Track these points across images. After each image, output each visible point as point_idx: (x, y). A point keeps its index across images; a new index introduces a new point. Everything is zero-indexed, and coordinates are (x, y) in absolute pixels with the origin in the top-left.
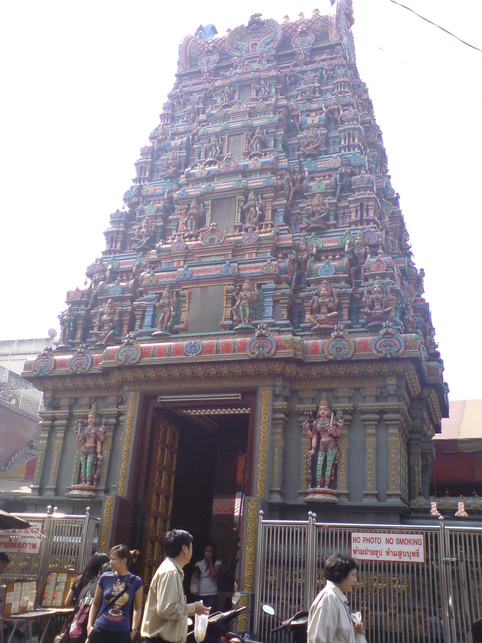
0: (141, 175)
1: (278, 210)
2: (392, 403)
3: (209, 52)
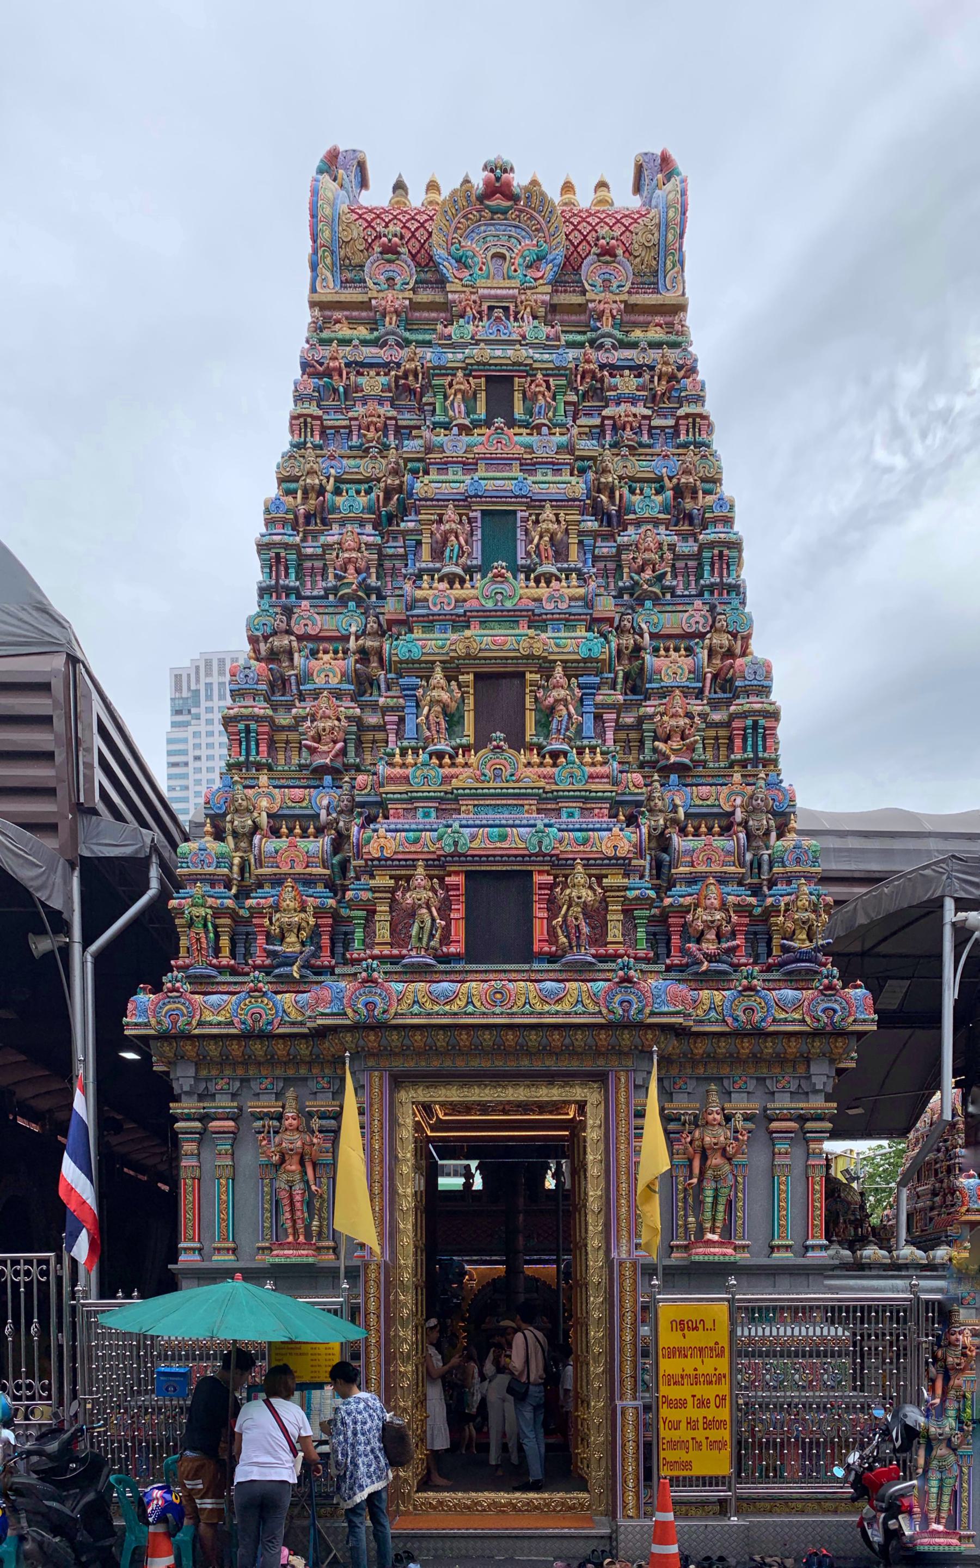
1: (605, 716)
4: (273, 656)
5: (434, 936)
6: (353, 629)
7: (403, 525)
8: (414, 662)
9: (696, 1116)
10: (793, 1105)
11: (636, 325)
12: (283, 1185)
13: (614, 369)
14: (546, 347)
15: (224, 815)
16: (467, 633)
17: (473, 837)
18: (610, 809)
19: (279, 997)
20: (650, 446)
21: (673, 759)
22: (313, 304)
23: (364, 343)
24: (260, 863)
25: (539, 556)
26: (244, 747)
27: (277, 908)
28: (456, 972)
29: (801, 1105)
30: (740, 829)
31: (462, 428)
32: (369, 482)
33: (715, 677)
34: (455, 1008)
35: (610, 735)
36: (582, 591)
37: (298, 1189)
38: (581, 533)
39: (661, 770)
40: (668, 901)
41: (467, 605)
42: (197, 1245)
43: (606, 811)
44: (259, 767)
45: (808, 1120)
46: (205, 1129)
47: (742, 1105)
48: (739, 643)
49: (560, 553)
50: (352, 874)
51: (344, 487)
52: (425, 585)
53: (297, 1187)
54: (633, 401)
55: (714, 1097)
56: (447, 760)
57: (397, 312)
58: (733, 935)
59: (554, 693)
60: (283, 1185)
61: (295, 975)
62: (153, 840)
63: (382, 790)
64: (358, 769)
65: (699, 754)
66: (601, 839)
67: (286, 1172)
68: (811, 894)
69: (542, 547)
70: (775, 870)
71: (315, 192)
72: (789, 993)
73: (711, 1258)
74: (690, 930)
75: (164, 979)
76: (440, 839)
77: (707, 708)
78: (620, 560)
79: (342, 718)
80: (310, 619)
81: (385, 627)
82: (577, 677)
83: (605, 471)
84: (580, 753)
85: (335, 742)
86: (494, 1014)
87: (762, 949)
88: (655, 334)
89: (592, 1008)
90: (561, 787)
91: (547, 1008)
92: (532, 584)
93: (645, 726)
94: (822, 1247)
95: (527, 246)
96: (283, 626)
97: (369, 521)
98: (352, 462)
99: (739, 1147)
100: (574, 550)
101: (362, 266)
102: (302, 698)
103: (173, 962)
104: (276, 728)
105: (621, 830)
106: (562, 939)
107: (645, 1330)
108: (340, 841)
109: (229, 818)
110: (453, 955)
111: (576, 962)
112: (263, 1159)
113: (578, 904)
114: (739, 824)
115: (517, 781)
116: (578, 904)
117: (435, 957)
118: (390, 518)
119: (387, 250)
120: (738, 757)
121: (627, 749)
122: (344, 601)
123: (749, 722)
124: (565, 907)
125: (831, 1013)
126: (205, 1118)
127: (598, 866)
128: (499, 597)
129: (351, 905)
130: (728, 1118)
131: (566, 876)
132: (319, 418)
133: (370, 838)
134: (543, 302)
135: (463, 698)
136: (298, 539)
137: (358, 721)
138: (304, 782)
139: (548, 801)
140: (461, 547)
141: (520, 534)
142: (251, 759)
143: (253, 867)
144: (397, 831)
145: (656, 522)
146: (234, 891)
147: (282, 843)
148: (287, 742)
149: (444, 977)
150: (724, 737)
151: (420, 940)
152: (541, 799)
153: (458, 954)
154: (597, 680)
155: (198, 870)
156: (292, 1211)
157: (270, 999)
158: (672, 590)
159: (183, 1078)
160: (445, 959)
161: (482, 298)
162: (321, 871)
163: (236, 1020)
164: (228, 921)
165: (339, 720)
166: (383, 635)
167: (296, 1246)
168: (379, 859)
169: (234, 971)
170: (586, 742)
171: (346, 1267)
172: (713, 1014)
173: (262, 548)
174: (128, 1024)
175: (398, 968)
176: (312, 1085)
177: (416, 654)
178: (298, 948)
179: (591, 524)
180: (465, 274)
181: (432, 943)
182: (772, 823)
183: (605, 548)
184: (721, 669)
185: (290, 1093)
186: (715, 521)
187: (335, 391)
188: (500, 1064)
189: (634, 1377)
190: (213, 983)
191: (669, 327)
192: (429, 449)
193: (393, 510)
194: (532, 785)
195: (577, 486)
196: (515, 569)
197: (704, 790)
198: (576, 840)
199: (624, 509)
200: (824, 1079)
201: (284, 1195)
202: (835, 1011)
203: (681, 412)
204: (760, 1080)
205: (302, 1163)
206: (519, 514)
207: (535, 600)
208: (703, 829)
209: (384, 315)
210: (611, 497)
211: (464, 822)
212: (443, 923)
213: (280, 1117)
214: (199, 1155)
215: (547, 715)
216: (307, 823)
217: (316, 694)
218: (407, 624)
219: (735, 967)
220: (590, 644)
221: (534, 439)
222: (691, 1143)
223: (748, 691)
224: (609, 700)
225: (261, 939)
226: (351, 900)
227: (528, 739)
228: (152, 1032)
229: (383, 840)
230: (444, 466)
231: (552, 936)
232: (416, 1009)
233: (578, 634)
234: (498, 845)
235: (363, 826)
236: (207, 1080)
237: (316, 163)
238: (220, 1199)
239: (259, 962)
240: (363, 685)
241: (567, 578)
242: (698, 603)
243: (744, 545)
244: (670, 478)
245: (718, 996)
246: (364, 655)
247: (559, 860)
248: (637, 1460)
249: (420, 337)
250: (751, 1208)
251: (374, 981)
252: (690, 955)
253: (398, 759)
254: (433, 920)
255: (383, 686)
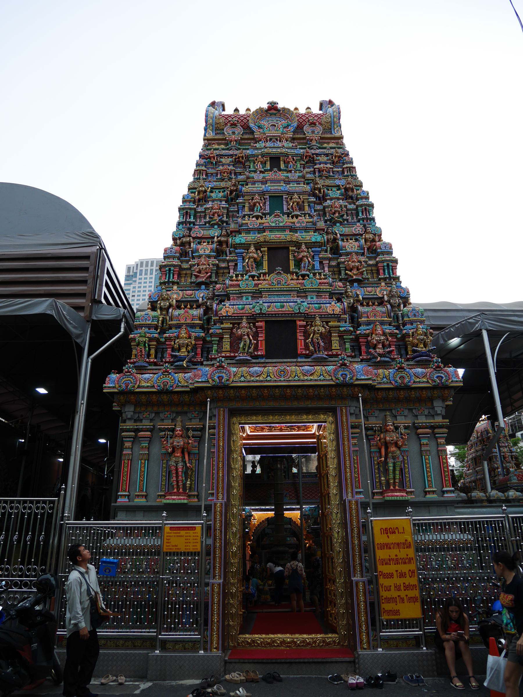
0: (186, 219)
2: (439, 420)
3: (234, 125)
4: (183, 244)
5: (251, 348)
6: (216, 234)
7: (237, 201)
8: (242, 244)
9: (380, 427)
10: (428, 421)
11: (325, 143)
12: (173, 463)
13: (317, 155)
14: (292, 148)
15: (157, 301)
16: (264, 234)
17: (269, 307)
18: (329, 296)
19: (177, 375)
20: (334, 176)
21: (354, 277)
22: (204, 140)
23: (223, 149)
24: (171, 319)
25: (293, 209)
26: (167, 276)
27: (178, 337)
28: (261, 363)
29: (432, 421)
30: (387, 303)
31: (261, 172)
32: (224, 189)
33: (368, 249)
34: (261, 378)
35: (326, 269)
36: (311, 220)
37: (180, 465)
38: (308, 202)
39: (349, 282)
40: (358, 332)
41: (264, 225)
42: (127, 493)
43: (328, 297)
44: (173, 283)
45: (436, 428)
46: (136, 435)
47: (402, 422)
48: (377, 237)
49: (301, 208)
50: (213, 323)
51: (214, 190)
52: (246, 219)
53: (180, 464)
54: (326, 163)
55: (389, 418)
56: (256, 278)
57: (236, 141)
58: (390, 346)
59: (302, 254)
60: (173, 463)
61: (185, 365)
62: (124, 312)
63: (227, 290)
64: (216, 283)
65: (365, 275)
66: (327, 307)
67: (175, 457)
68: (423, 328)
69: (294, 206)
70: (405, 319)
71: (207, 111)
72: (420, 370)
73: (396, 498)
74: (370, 344)
75: (124, 368)
76: (254, 307)
77: (367, 260)
78: (325, 211)
79: (210, 264)
80: (198, 232)
81: (229, 233)
82: (311, 248)
83: (317, 184)
84: (314, 274)
85: (207, 273)
86: (280, 381)
87: (403, 352)
88: (332, 145)
89: (328, 378)
90: (307, 287)
91: (306, 378)
92: (290, 218)
93: (341, 266)
94: (451, 491)
95: (284, 122)
96: (187, 234)
97: (224, 200)
98: (218, 183)
99: (403, 442)
100: (307, 208)
101: (223, 129)
102: (193, 258)
103: (128, 361)
104: (181, 268)
105: (335, 303)
106: (311, 348)
107: (364, 538)
108: (208, 310)
109: (159, 302)
110: (259, 355)
111: (318, 358)
112: (164, 451)
113: (318, 333)
114: (386, 302)
115: (288, 285)
116: (318, 333)
117: (251, 357)
118: (232, 199)
119: (232, 125)
120: (382, 277)
121: (334, 273)
122: (212, 226)
123: (385, 264)
124: (312, 335)
125: (441, 378)
126: (137, 431)
127: (326, 318)
128: (277, 222)
129: (212, 335)
130: (397, 428)
131: (312, 322)
132: (206, 171)
133: (222, 308)
134: (290, 137)
135: (262, 256)
136: (195, 206)
137: (217, 266)
138: (193, 288)
139: (302, 293)
140: (261, 207)
141: (284, 203)
142: (171, 280)
143: (168, 321)
144: (234, 305)
145: (338, 199)
146: (158, 331)
147: (182, 311)
148: (186, 274)
149: (255, 365)
150: (376, 270)
151: (244, 349)
152: (298, 292)
153: (262, 355)
154: (320, 249)
155: (144, 323)
156: (177, 477)
157: (172, 376)
158: (347, 220)
159: (129, 411)
160: (257, 357)
161: (268, 136)
162: (198, 322)
163: (156, 385)
164: (155, 343)
165: (209, 265)
166: (229, 236)
167: (178, 494)
168: (225, 316)
169: (155, 364)
170: (316, 271)
171: (205, 505)
172: (385, 380)
173: (180, 209)
174: (105, 387)
175: (234, 361)
176: (190, 415)
177: (243, 241)
178: (186, 354)
179: (313, 199)
180: (261, 131)
181: (250, 350)
182: (401, 301)
183: (319, 207)
184: (370, 246)
185: (179, 419)
186: (362, 198)
187: (212, 163)
188: (284, 405)
189: (361, 564)
190: (146, 369)
191: (337, 143)
192: (248, 178)
193: (233, 197)
194: (295, 286)
195: (308, 188)
196: (284, 214)
197: (369, 289)
198: (315, 307)
199: (325, 195)
200: (441, 408)
201: (173, 468)
202: (442, 377)
203: (345, 166)
204: (410, 410)
205: (183, 453)
206: (284, 197)
207: (292, 223)
208: (371, 304)
209: (231, 142)
210: (320, 192)
211: (264, 301)
212: (255, 342)
213: (173, 430)
214: (132, 448)
215: (298, 262)
216: (194, 304)
217: (200, 257)
218: (239, 232)
219: (393, 359)
220: (316, 237)
221: (289, 175)
222: (379, 440)
223: (383, 253)
224: (325, 256)
225: (169, 350)
226: (212, 333)
227: (291, 270)
228: (116, 390)
229: (228, 308)
230: (254, 183)
231: (307, 347)
232: (242, 379)
233: (310, 234)
234: (280, 310)
235: (218, 304)
236: (139, 413)
237: (208, 105)
238: (141, 470)
239: (168, 360)
240: (219, 253)
241: (304, 216)
242: (358, 224)
243: (374, 206)
244: (343, 186)
245: (386, 372)
246: (220, 243)
247: (308, 315)
248: (366, 613)
249: (244, 147)
250: (413, 470)
251: (223, 367)
252: (372, 354)
253: (234, 278)
254: (250, 341)
255: (228, 253)
